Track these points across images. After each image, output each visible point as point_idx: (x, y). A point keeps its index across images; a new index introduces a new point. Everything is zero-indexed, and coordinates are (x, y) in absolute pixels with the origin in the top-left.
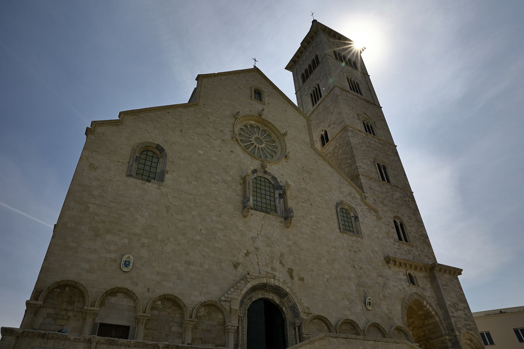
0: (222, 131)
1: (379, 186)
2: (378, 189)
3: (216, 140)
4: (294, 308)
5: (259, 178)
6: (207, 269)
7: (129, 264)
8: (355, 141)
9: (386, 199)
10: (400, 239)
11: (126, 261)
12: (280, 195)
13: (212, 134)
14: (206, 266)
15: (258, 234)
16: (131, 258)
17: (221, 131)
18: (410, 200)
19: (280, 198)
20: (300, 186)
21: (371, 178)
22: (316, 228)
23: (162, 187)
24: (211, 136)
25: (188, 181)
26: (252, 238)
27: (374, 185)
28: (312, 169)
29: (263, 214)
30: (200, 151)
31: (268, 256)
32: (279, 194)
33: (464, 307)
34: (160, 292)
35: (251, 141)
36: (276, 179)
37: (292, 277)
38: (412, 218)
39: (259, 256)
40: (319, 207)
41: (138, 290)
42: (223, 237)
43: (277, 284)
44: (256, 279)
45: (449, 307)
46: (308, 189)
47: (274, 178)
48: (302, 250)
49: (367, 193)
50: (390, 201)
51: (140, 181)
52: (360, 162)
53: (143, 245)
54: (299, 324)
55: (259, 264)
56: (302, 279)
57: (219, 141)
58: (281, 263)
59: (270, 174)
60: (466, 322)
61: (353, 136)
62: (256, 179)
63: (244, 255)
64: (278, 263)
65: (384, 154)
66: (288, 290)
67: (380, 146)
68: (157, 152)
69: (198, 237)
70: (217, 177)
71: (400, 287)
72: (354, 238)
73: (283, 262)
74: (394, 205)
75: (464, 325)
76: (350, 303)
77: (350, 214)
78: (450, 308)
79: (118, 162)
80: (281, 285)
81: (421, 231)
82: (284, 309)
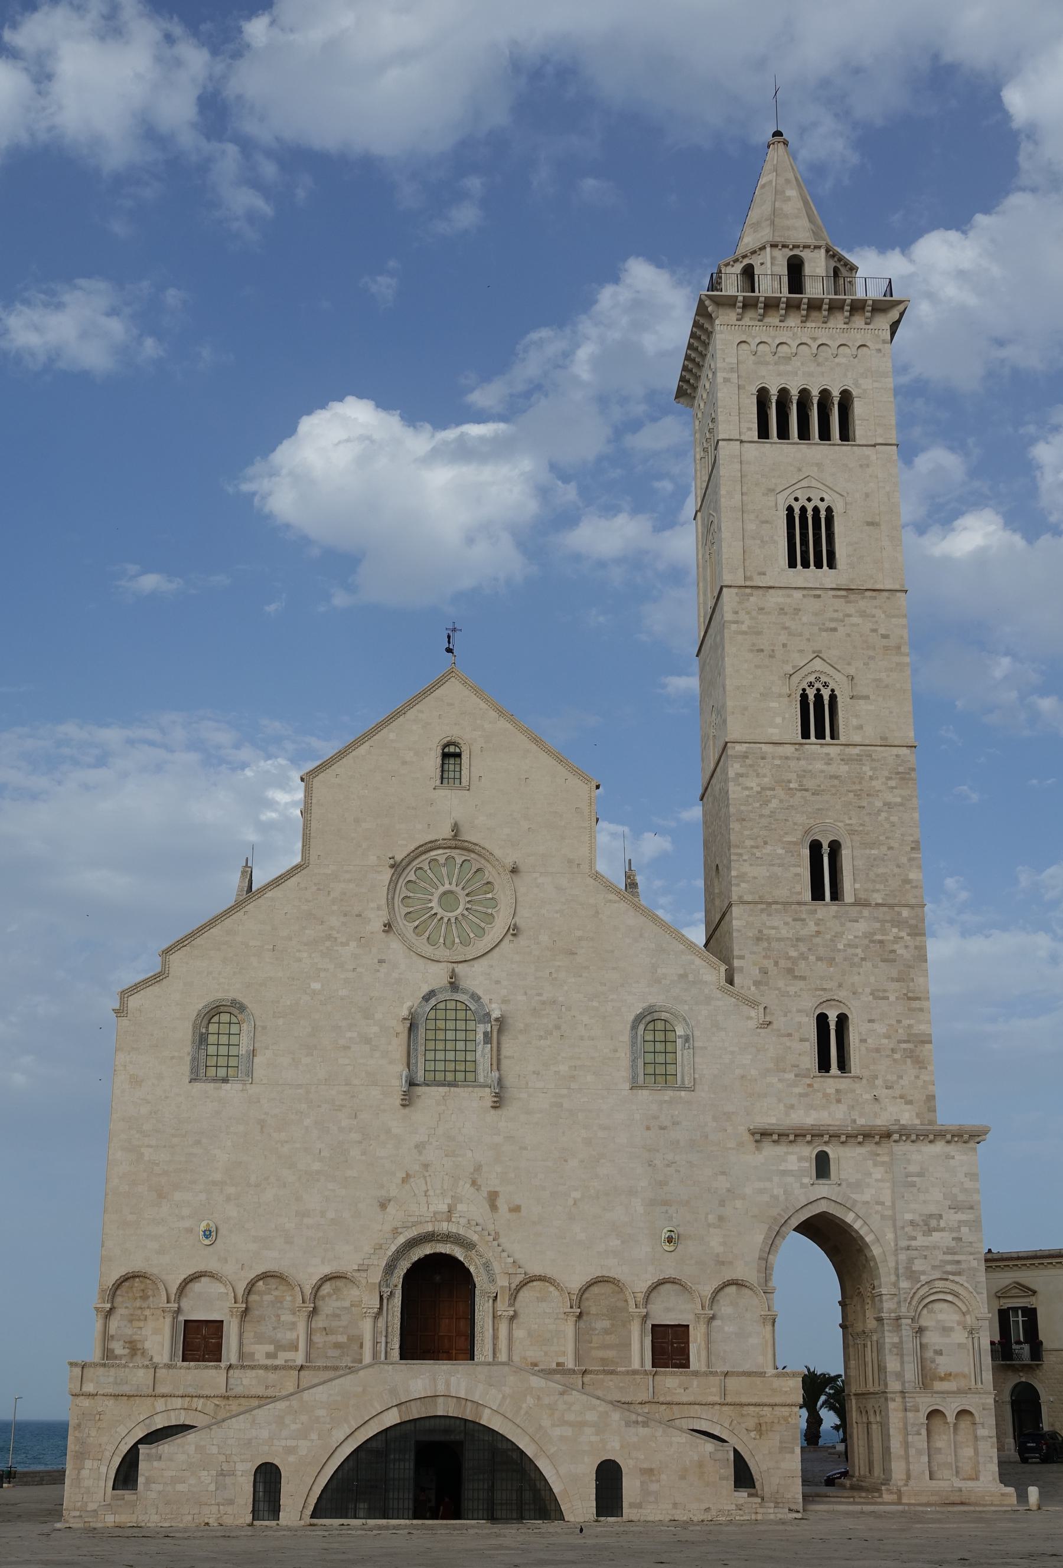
0: (360, 915)
1: (795, 920)
2: (788, 932)
3: (347, 944)
4: (487, 1266)
5: (442, 1006)
6: (332, 1219)
7: (210, 1234)
8: (747, 788)
9: (806, 959)
10: (824, 1065)
11: (204, 1232)
12: (486, 1034)
13: (338, 933)
14: (331, 1215)
15: (429, 1135)
16: (212, 1224)
17: (357, 916)
18: (903, 934)
19: (485, 1043)
20: (538, 998)
21: (770, 904)
22: (565, 1092)
23: (248, 1086)
24: (336, 938)
25: (293, 1059)
26: (417, 1147)
27: (776, 924)
28: (580, 939)
29: (442, 1090)
30: (316, 986)
31: (447, 1174)
32: (484, 1033)
33: (960, 1222)
34: (260, 1269)
35: (432, 908)
36: (480, 998)
37: (494, 1207)
38: (887, 994)
39: (428, 1179)
40: (582, 1038)
41: (228, 1270)
42: (362, 1155)
43: (454, 1231)
44: (414, 1228)
45: (903, 1228)
46: (560, 999)
47: (476, 998)
48: (525, 1149)
49: (742, 957)
50: (819, 959)
51: (212, 1084)
52: (745, 861)
53: (228, 1199)
54: (495, 1295)
55: (428, 1193)
56: (516, 1209)
57: (353, 944)
58: (474, 1183)
59: (465, 992)
60: (949, 1257)
61: (742, 775)
62: (436, 1009)
63: (400, 1181)
64: (468, 1186)
65: (851, 795)
66: (475, 1238)
67: (844, 769)
68: (236, 1012)
69: (316, 1166)
70: (349, 1035)
71: (778, 1191)
72: (668, 1095)
73: (479, 1182)
74: (832, 969)
75: (937, 1263)
76: (623, 1242)
77: (675, 1031)
78: (909, 1229)
79: (173, 1058)
80: (461, 1232)
81: (910, 1026)
82: (472, 1269)
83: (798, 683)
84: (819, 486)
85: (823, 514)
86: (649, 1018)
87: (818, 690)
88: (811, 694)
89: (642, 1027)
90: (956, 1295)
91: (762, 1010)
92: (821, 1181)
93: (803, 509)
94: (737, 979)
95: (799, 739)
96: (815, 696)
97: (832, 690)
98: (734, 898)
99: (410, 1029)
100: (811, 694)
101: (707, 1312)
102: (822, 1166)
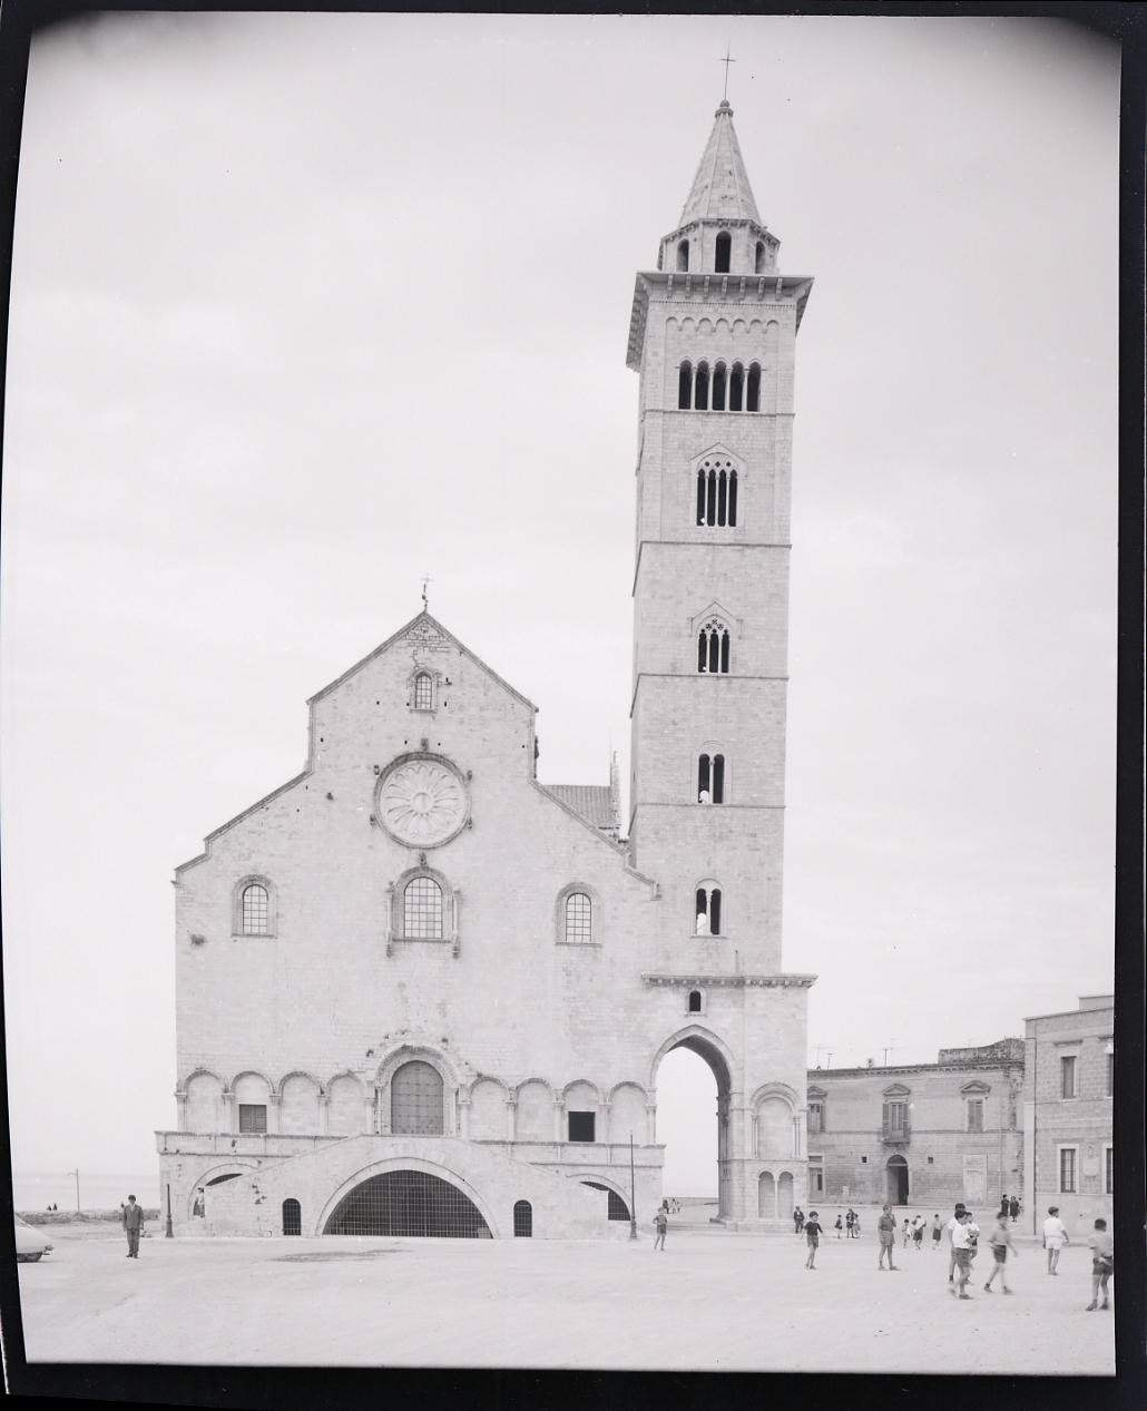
83: (699, 625)
84: (728, 453)
85: (728, 476)
86: (570, 893)
87: (715, 631)
88: (709, 634)
89: (565, 898)
90: (786, 1094)
91: (655, 886)
92: (693, 1013)
93: (713, 473)
94: (639, 864)
95: (696, 672)
96: (712, 636)
97: (726, 631)
98: (639, 801)
99: (393, 899)
100: (709, 634)
101: (607, 1103)
102: (695, 1003)
